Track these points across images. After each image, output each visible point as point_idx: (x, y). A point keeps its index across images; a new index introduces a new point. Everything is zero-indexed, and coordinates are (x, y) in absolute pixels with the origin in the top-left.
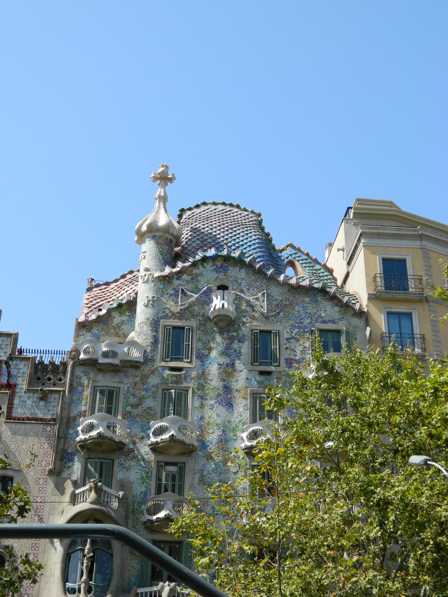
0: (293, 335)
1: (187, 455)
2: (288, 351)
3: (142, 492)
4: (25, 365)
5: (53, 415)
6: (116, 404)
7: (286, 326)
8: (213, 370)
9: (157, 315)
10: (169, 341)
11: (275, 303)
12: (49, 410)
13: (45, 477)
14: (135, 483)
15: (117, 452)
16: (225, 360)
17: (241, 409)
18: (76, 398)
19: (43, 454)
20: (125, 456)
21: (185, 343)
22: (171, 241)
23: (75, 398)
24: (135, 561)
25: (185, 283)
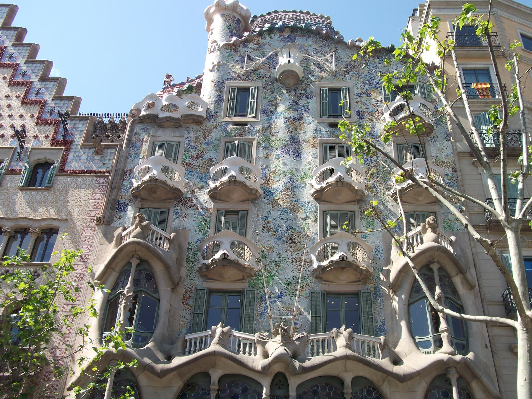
0: (364, 91)
1: (250, 202)
2: (359, 105)
3: (198, 240)
4: (83, 124)
5: (108, 168)
6: (175, 157)
7: (357, 83)
8: (280, 123)
9: (222, 77)
10: (234, 99)
11: (343, 64)
12: (104, 164)
13: (93, 227)
14: (192, 231)
15: (172, 201)
16: (291, 114)
17: (310, 158)
18: (133, 153)
19: (93, 204)
20: (182, 205)
21: (250, 101)
22: (239, 20)
23: (132, 152)
24: (187, 312)
25: (251, 50)
